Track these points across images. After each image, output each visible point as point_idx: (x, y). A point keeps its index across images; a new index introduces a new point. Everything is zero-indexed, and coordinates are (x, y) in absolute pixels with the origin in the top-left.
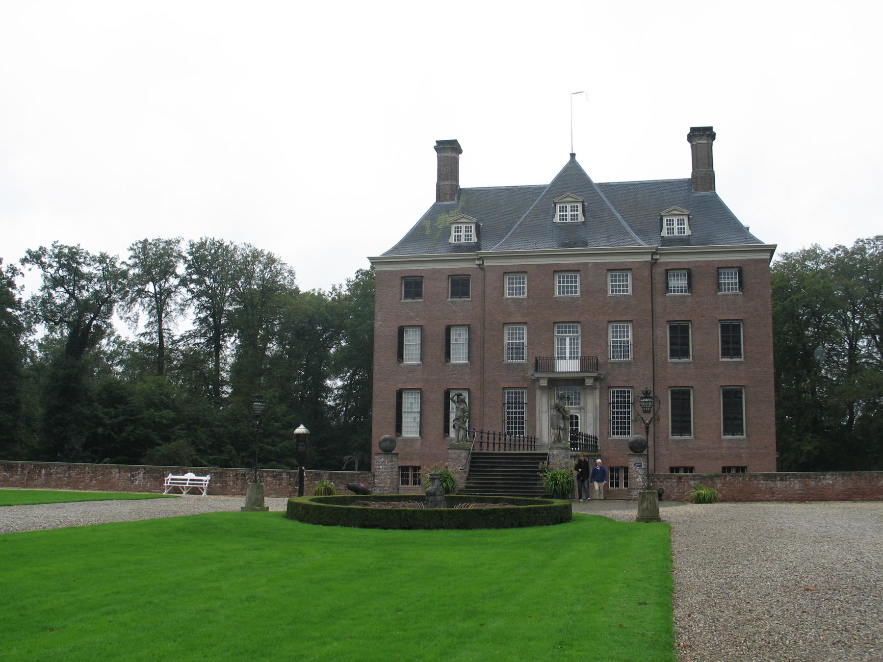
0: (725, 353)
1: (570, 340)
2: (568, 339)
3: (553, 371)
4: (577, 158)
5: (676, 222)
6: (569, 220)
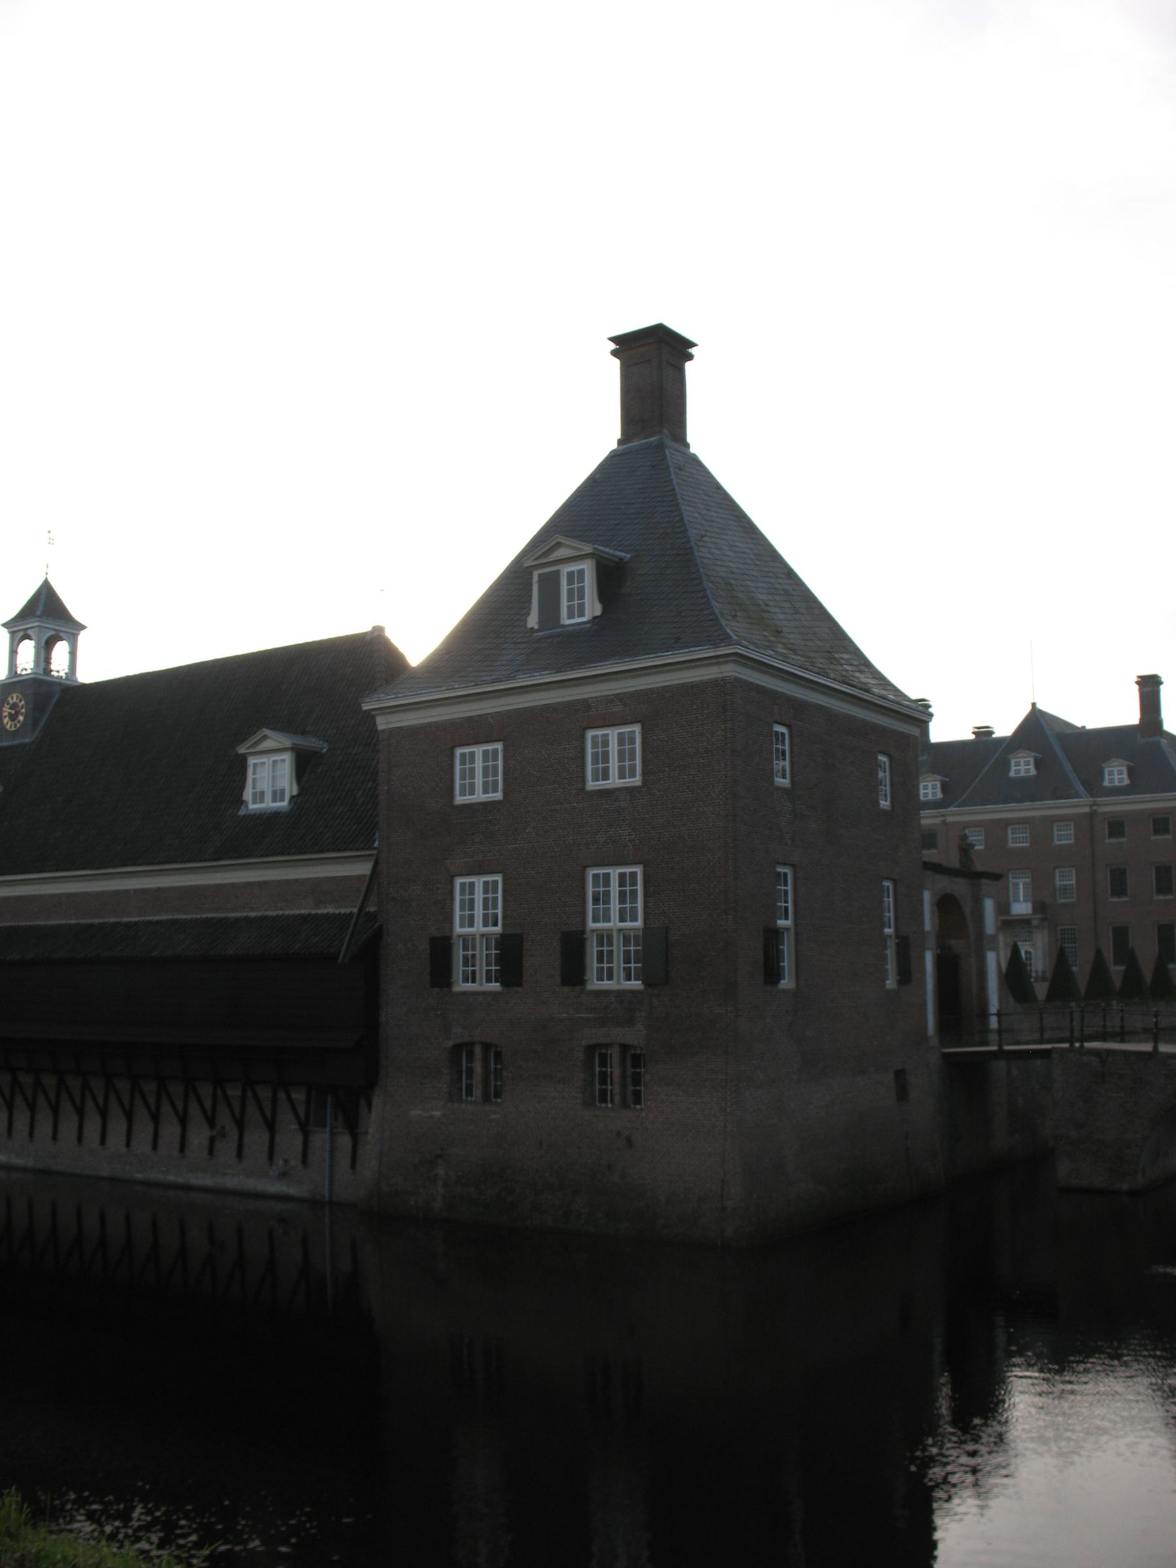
0: (1159, 891)
4: (1039, 706)
5: (1116, 773)
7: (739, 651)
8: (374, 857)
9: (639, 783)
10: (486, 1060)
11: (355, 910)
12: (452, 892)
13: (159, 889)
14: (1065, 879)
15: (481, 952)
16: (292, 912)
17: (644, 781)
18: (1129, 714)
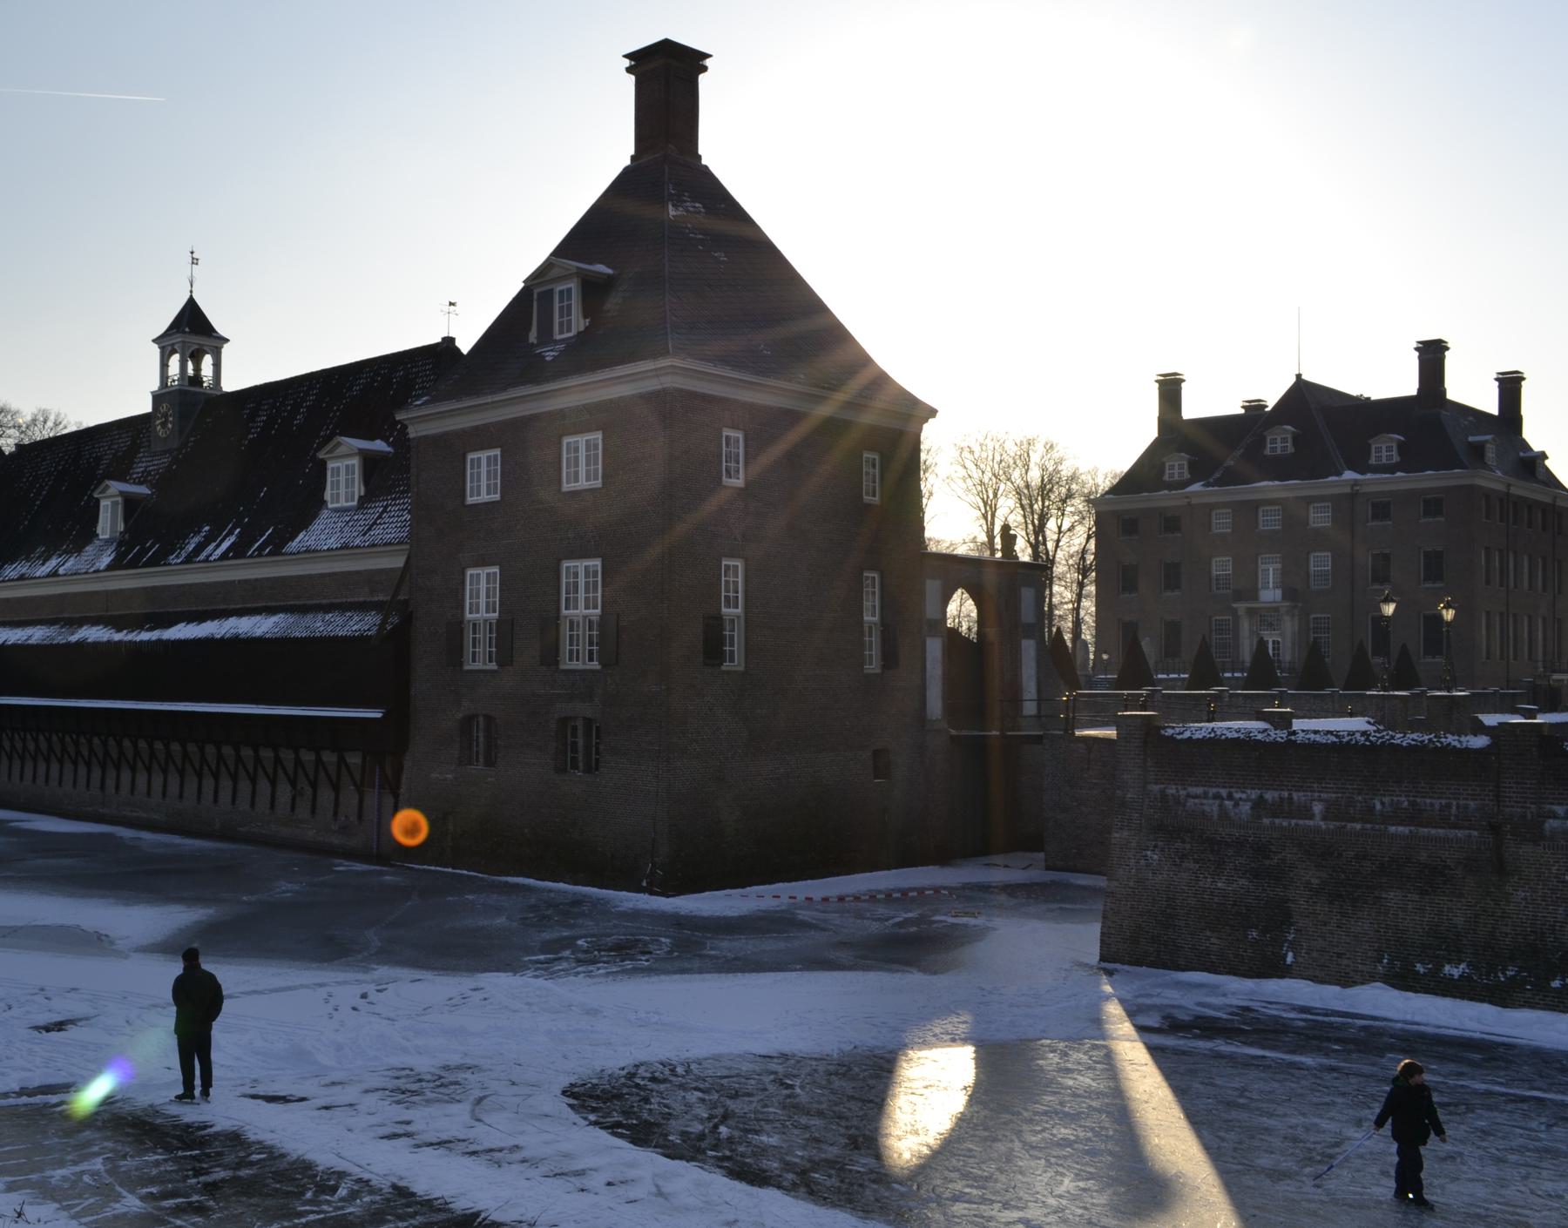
1: (1274, 570)
2: (1271, 569)
3: (1255, 598)
4: (1303, 377)
5: (1384, 450)
6: (1279, 452)
7: (674, 364)
8: (407, 552)
9: (600, 486)
10: (588, 734)
11: (389, 598)
12: (463, 582)
13: (256, 580)
14: (1320, 562)
15: (583, 633)
16: (352, 600)
17: (603, 483)
18: (1406, 383)
